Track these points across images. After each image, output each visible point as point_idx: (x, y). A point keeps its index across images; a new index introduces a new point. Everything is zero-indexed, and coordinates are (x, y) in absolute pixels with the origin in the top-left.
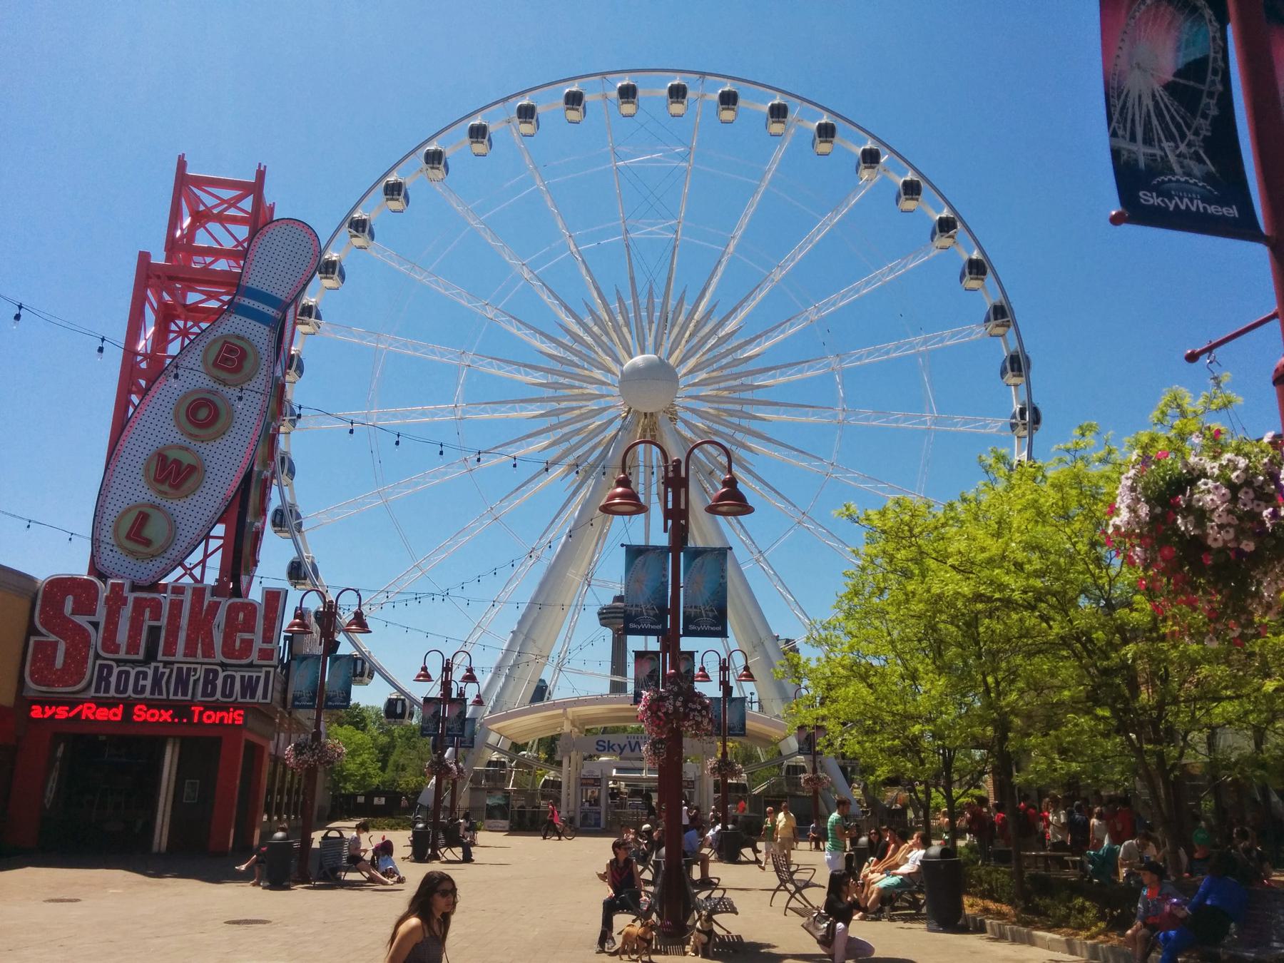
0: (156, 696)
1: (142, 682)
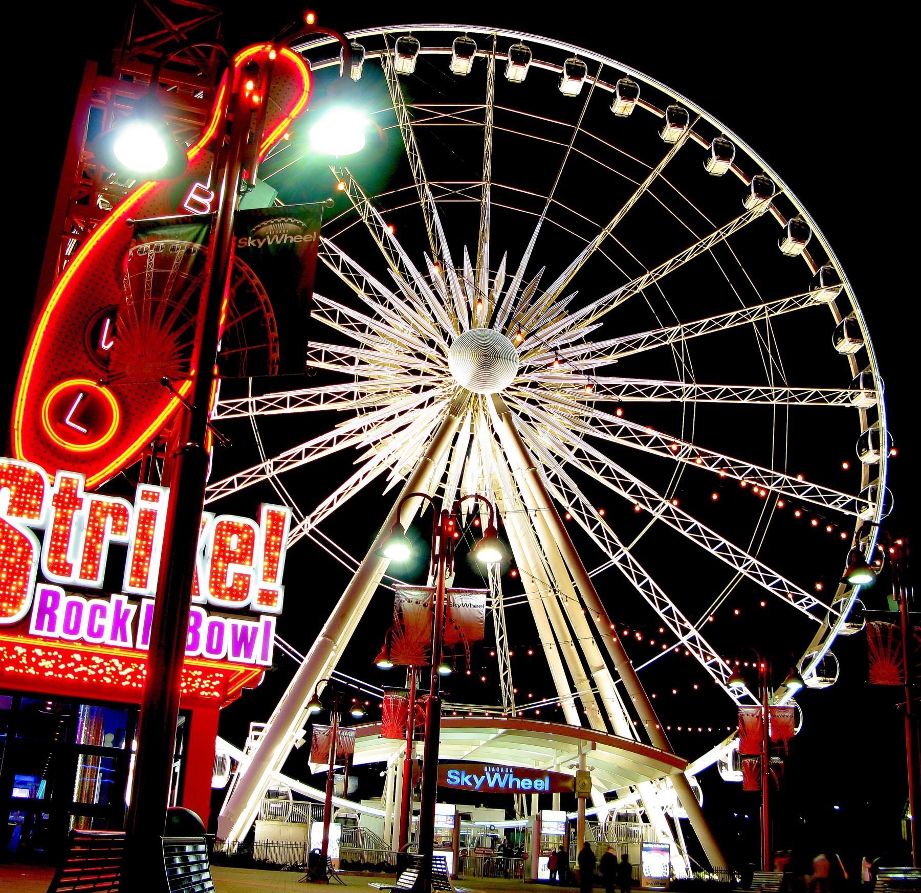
0: (118, 642)
1: (98, 621)
